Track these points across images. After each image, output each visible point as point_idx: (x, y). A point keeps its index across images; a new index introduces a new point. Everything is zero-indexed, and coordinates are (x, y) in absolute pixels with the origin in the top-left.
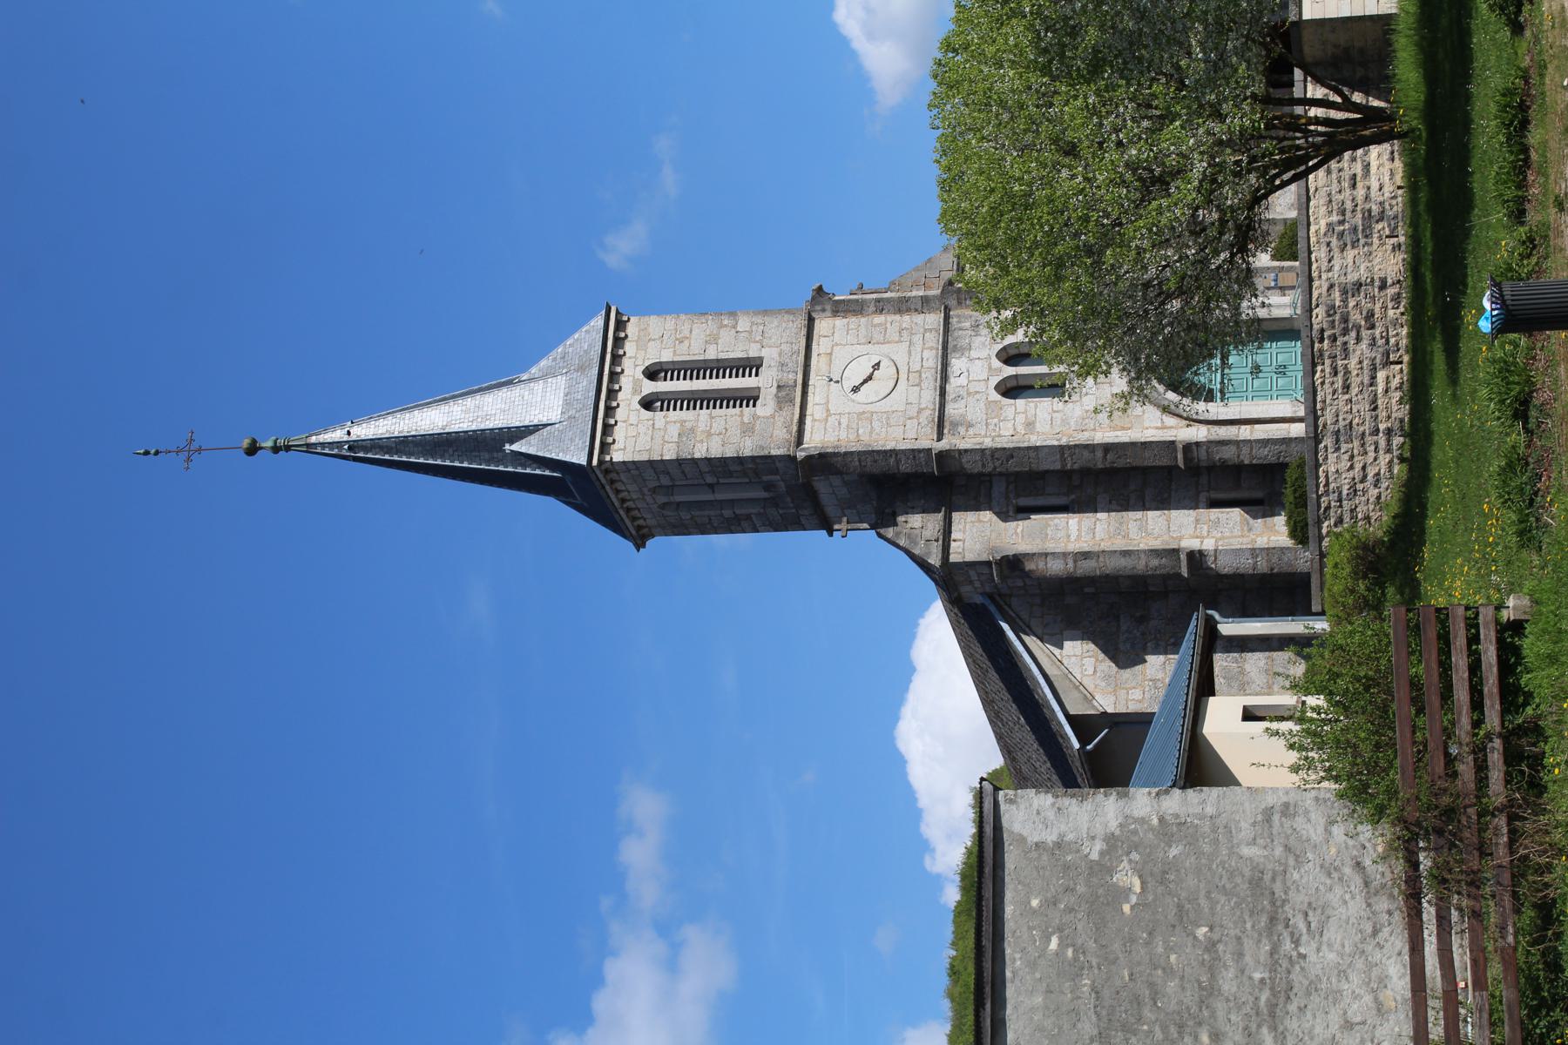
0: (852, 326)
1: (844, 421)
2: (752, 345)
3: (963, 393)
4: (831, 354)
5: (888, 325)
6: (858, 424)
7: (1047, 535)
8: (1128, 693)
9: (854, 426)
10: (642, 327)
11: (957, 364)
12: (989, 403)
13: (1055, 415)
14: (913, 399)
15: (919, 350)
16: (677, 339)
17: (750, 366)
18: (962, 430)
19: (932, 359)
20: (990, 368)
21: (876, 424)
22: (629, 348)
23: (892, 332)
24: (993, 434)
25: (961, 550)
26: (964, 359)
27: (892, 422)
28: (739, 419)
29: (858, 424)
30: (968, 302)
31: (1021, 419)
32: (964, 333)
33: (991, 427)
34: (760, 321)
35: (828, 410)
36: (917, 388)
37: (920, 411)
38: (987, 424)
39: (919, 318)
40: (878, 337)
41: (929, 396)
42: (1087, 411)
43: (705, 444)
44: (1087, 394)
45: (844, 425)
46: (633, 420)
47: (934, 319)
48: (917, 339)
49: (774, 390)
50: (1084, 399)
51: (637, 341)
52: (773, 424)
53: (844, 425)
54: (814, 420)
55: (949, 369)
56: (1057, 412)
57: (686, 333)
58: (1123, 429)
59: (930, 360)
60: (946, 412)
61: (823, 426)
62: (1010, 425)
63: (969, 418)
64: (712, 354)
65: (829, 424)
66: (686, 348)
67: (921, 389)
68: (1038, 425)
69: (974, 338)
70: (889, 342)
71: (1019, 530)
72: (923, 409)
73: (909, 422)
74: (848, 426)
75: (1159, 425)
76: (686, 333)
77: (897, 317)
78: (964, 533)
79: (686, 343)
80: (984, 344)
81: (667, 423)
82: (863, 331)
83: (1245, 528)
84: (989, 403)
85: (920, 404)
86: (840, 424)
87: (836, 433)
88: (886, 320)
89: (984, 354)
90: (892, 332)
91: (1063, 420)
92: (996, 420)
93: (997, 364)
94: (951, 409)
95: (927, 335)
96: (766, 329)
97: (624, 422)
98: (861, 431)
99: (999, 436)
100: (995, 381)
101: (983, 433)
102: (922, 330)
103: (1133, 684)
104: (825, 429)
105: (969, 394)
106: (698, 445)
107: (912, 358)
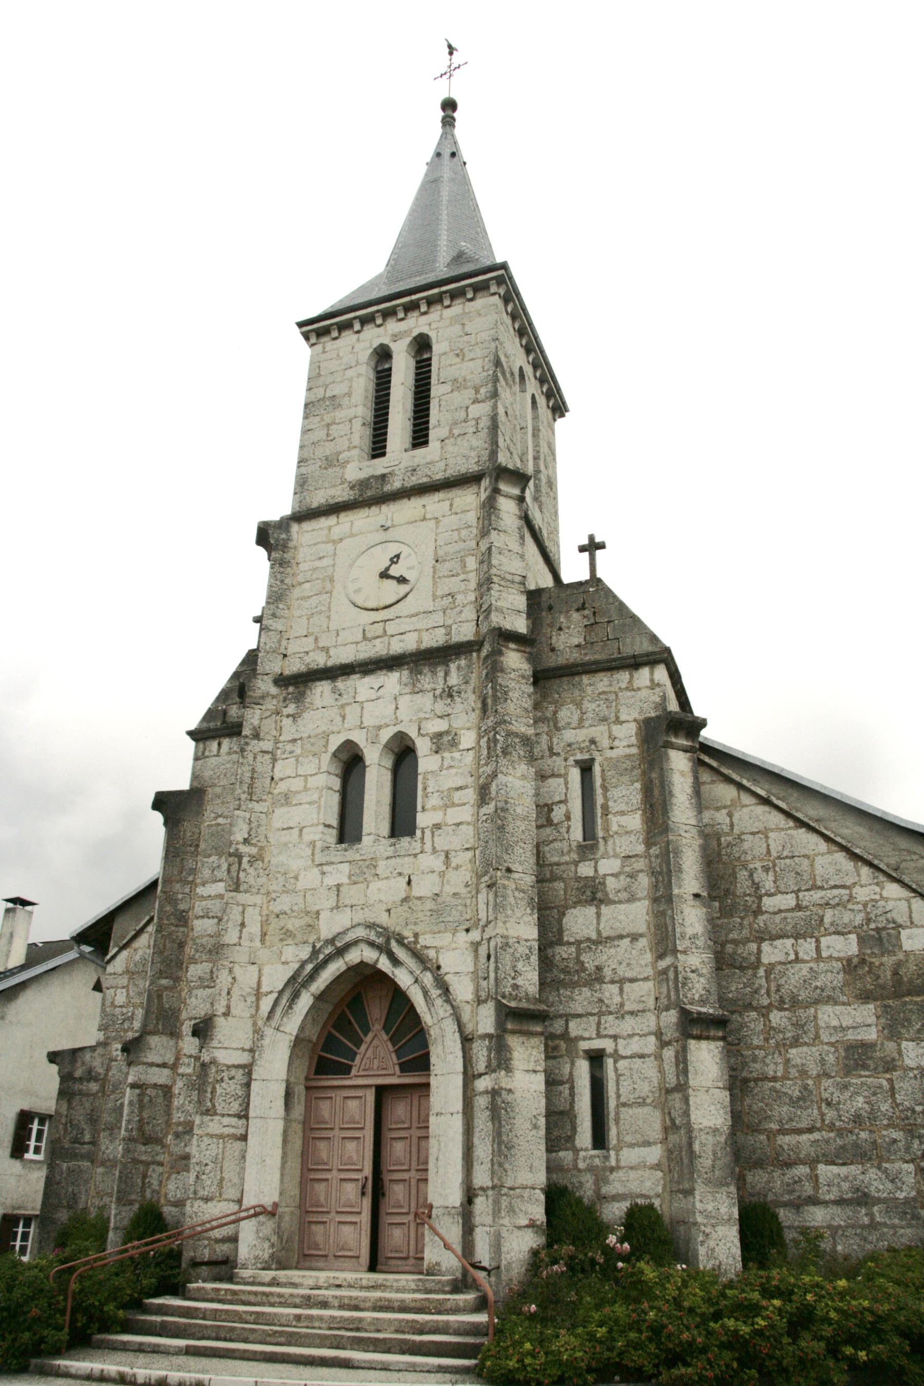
0: (464, 533)
1: (326, 562)
2: (447, 428)
3: (345, 699)
4: (424, 519)
5: (462, 577)
6: (317, 579)
7: (209, 856)
8: (123, 987)
9: (315, 576)
10: (482, 312)
11: (392, 680)
12: (326, 736)
13: (296, 832)
14: (344, 637)
15: (419, 627)
16: (462, 350)
17: (420, 437)
18: (291, 708)
19: (397, 647)
20: (379, 728)
21: (314, 601)
22: (458, 308)
23: (453, 584)
24: (279, 752)
25: (207, 753)
26: (397, 689)
27: (315, 620)
28: (346, 447)
29: (317, 579)
30: (484, 673)
31: (297, 785)
32: (441, 680)
33: (289, 747)
34: (480, 426)
35: (341, 540)
36: (360, 637)
37: (326, 650)
38: (294, 741)
39: (470, 614)
40: (444, 569)
41: (344, 655)
42: (296, 878)
43: (316, 426)
44: (323, 873)
45: (318, 564)
46: (359, 347)
47: (465, 632)
48: (438, 619)
49: (380, 471)
50: (316, 871)
51: (464, 313)
52: (335, 486)
53: (318, 564)
54: (330, 528)
55: (384, 672)
56: (301, 835)
57: (472, 355)
58: (264, 935)
59: (402, 644)
60: (318, 683)
61: (319, 540)
62: (290, 772)
63: (305, 715)
64: (436, 391)
65: (322, 546)
66: (449, 362)
67: (357, 643)
68: (284, 809)
69: (431, 694)
70: (435, 583)
71: (220, 820)
72: (327, 652)
73: (311, 639)
74: (317, 568)
75: (264, 989)
76: (469, 356)
77: (473, 585)
78: (229, 754)
79: (457, 360)
80: (420, 710)
81: (351, 380)
82: (451, 549)
83: (180, 1129)
84: (326, 736)
85: (335, 646)
86: (320, 558)
87: (307, 559)
88: (467, 573)
89: (403, 714)
90: (453, 584)
91: (286, 844)
92: (298, 751)
93: (386, 735)
94: (321, 691)
95: (442, 630)
96: (467, 437)
97: (358, 340)
98: (307, 585)
99: (274, 760)
100: (359, 738)
101: (282, 738)
102: (449, 622)
103: (132, 994)
104: (315, 544)
105: (342, 707)
106: (318, 418)
107: (407, 620)
